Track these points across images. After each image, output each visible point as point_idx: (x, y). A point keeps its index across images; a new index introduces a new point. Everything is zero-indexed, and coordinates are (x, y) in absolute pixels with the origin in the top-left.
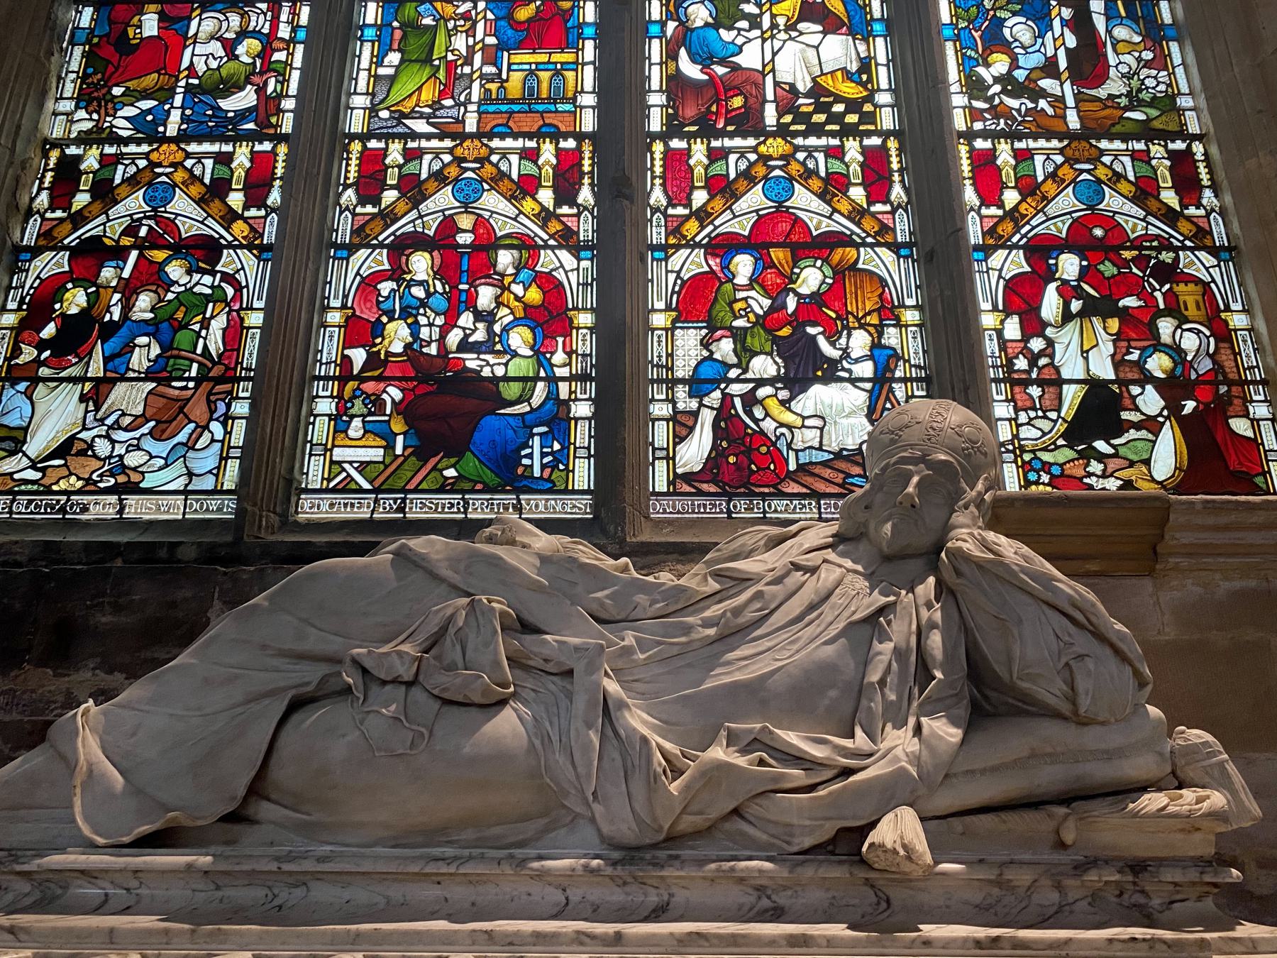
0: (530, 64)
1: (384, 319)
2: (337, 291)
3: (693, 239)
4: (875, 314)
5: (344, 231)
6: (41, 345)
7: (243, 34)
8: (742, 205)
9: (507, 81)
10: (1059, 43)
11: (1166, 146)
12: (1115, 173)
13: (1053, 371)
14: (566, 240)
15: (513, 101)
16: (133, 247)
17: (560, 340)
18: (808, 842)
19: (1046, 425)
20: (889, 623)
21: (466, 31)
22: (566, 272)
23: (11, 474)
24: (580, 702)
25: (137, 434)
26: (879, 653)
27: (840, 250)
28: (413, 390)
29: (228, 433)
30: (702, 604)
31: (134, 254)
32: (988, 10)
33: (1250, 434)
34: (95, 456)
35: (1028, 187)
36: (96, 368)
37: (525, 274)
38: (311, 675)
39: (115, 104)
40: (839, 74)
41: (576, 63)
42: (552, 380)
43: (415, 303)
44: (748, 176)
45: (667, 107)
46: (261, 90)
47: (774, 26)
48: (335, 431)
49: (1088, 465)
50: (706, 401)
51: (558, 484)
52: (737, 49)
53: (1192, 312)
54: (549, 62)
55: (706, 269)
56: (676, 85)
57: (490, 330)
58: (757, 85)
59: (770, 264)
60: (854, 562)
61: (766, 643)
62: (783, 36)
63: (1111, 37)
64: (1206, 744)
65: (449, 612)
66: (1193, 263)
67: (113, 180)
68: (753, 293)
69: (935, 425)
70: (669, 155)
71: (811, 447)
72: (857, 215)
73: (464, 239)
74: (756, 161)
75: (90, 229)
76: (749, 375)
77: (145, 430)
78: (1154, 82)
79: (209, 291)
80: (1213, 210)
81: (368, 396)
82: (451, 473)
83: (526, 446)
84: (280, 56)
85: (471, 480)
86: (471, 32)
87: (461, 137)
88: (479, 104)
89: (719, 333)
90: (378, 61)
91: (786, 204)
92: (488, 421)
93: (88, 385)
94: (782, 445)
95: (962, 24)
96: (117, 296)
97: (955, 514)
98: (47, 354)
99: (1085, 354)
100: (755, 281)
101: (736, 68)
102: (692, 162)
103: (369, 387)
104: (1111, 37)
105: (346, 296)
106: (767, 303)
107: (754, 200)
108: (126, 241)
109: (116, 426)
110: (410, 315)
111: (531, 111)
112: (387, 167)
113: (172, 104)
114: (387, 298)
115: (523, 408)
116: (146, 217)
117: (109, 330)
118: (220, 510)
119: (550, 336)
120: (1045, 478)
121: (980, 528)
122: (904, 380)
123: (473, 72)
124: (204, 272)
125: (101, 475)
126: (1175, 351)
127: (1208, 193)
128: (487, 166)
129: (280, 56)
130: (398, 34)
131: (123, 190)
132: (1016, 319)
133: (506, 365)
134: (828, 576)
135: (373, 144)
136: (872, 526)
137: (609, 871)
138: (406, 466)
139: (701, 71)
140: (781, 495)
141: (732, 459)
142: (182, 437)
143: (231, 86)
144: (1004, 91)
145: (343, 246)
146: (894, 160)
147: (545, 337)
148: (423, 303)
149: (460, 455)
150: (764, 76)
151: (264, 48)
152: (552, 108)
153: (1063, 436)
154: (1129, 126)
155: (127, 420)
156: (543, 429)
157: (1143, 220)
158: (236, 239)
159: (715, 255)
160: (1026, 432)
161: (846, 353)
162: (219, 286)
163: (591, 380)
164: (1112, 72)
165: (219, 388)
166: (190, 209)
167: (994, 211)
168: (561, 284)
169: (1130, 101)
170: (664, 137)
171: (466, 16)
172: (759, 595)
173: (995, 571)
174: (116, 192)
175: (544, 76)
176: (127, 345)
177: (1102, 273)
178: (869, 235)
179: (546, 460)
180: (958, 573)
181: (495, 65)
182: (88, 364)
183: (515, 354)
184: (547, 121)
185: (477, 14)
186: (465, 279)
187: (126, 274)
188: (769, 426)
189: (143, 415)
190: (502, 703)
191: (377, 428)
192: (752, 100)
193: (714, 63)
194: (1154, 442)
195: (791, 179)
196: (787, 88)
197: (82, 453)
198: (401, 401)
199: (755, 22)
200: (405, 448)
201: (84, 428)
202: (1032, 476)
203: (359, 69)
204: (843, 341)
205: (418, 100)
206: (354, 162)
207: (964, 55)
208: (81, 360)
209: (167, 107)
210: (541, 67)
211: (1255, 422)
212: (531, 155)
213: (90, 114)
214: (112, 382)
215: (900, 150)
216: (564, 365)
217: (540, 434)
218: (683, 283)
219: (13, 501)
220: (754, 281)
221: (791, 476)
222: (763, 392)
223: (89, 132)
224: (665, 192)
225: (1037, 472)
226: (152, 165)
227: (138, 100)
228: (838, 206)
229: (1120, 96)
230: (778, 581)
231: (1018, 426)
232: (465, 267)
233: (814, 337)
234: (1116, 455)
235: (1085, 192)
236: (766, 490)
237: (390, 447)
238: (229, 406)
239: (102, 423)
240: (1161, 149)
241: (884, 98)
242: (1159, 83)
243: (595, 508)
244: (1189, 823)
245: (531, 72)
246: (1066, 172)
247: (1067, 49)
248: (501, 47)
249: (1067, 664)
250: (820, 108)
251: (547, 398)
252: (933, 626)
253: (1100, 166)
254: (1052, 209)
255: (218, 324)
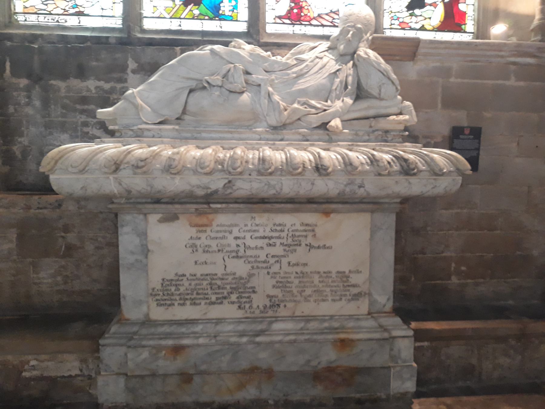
18: (315, 126)
20: (339, 73)
24: (263, 93)
26: (336, 82)
30: (292, 67)
38: (193, 84)
51: (234, 17)
60: (333, 56)
61: (308, 79)
64: (409, 105)
65: (228, 68)
69: (359, 15)
85: (203, 15)
97: (360, 43)
121: (367, 48)
134: (325, 60)
136: (338, 46)
137: (271, 131)
138: (180, 9)
172: (307, 65)
173: (367, 61)
180: (358, 61)
190: (243, 92)
230: (312, 61)
243: (249, 27)
244: (400, 122)
249: (380, 86)
252: (350, 75)
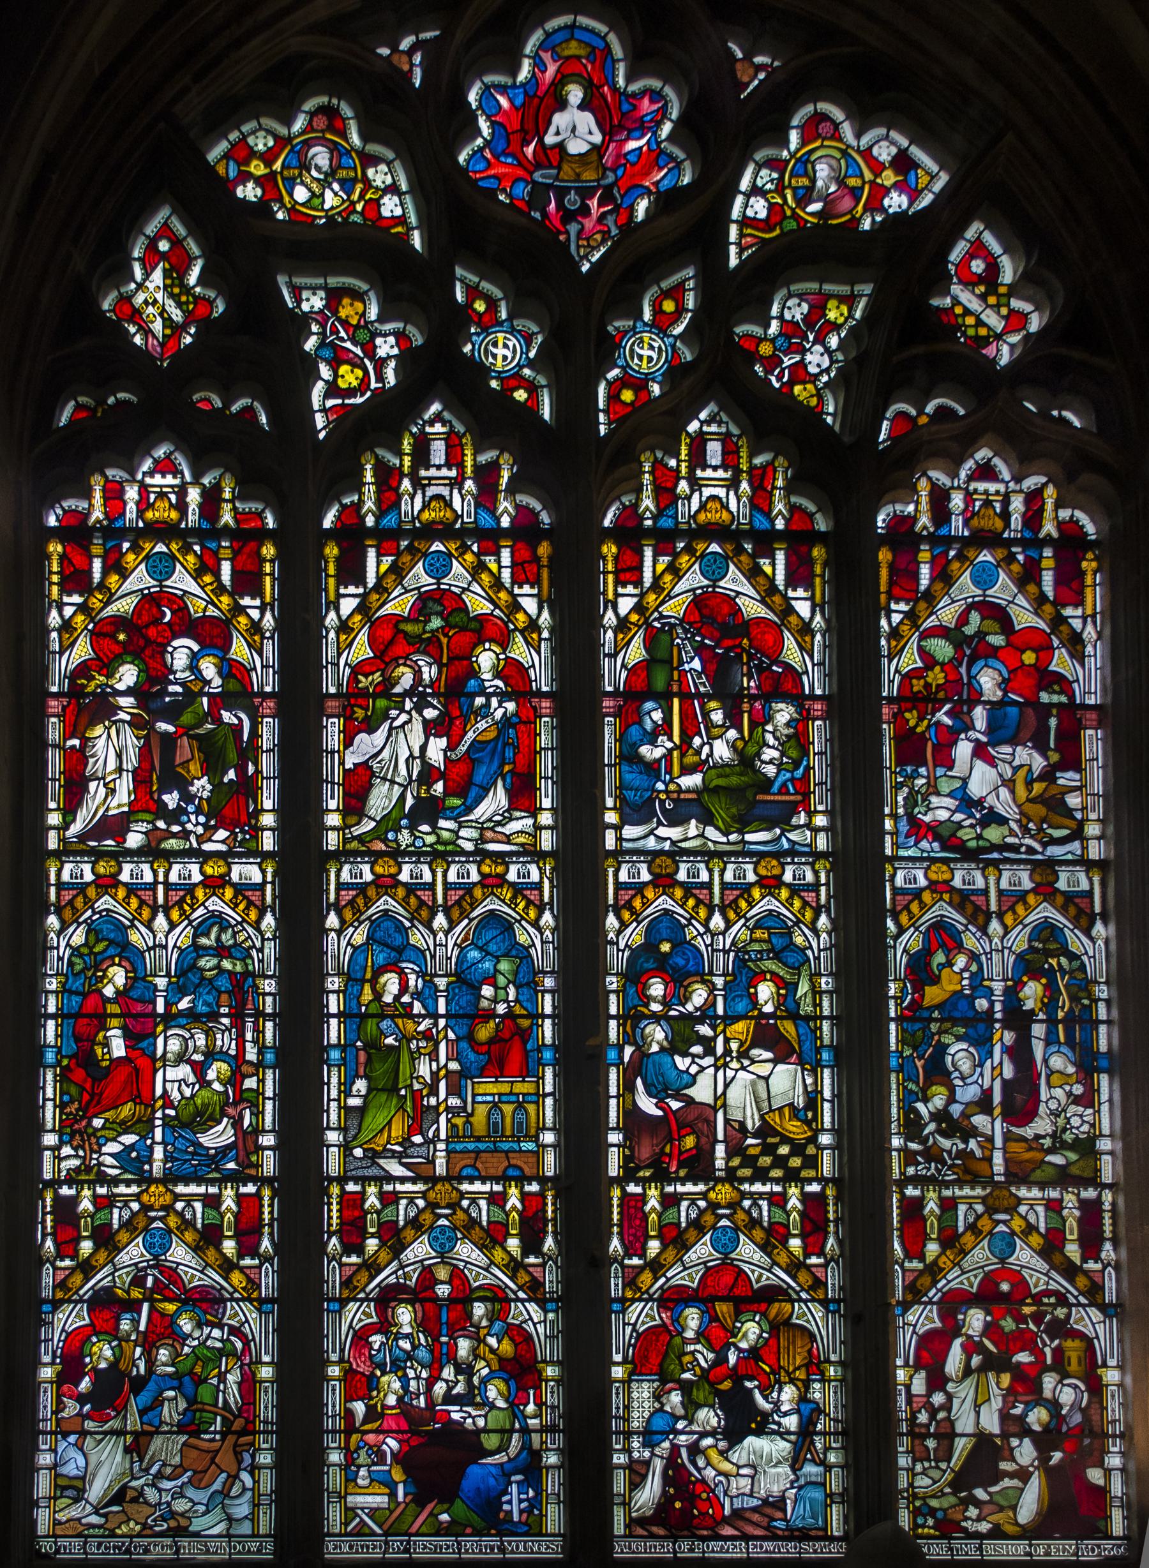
0: (493, 1095)
1: (378, 1373)
2: (334, 1343)
3: (647, 1292)
4: (803, 1369)
5: (334, 1282)
6: (81, 1399)
7: (211, 1054)
8: (691, 1256)
9: (472, 1115)
10: (996, 1072)
11: (1078, 1195)
12: (1028, 1224)
13: (948, 1424)
14: (534, 1292)
15: (478, 1139)
16: (144, 1300)
17: (532, 1392)
19: (936, 1474)
21: (429, 1054)
22: (535, 1324)
23: (79, 1520)
25: (179, 1482)
27: (776, 1305)
28: (407, 1441)
29: (256, 1482)
31: (146, 1306)
32: (933, 1034)
33: (1101, 1482)
34: (147, 1503)
35: (949, 1239)
36: (133, 1421)
37: (498, 1326)
39: (98, 1138)
40: (786, 1110)
41: (537, 1094)
42: (525, 1431)
43: (402, 1355)
44: (698, 1226)
45: (624, 1147)
46: (237, 1123)
47: (727, 1052)
48: (347, 1480)
49: (966, 1510)
50: (657, 1451)
52: (690, 1079)
53: (1074, 1367)
54: (511, 1093)
55: (658, 1322)
56: (633, 1118)
57: (469, 1382)
58: (707, 1121)
59: (714, 1318)
62: (735, 1065)
63: (1047, 1066)
66: (1082, 1318)
67: (111, 1224)
68: (699, 1347)
70: (625, 1197)
71: (743, 1494)
72: (795, 1267)
73: (443, 1290)
74: (706, 1209)
75: (102, 1279)
76: (695, 1428)
77: (185, 1479)
78: (1079, 1121)
79: (219, 1345)
80: (1109, 1264)
81: (371, 1447)
82: (445, 1517)
83: (505, 1492)
84: (250, 1083)
86: (434, 1056)
87: (432, 1180)
88: (447, 1141)
89: (669, 1385)
90: (346, 1090)
91: (733, 1256)
92: (473, 1470)
93: (129, 1439)
94: (720, 1491)
95: (907, 1053)
96: (138, 1350)
98: (87, 1407)
99: (977, 1407)
100: (702, 1335)
101: (690, 1101)
102: (647, 1208)
103: (371, 1438)
104: (1047, 1066)
105: (342, 1350)
106: (711, 1356)
107: (702, 1251)
108: (136, 1294)
109: (159, 1475)
110: (400, 1368)
111: (496, 1151)
112: (367, 1212)
113: (153, 1138)
114: (379, 1351)
115: (501, 1458)
116: (149, 1267)
117: (139, 1385)
118: (259, 1552)
119: (522, 1389)
120: (930, 1522)
122: (824, 1434)
123: (439, 1104)
124: (213, 1325)
125: (154, 1520)
126: (1054, 1405)
127: (1108, 1246)
128: (459, 1212)
129: (250, 1083)
130: (362, 1056)
131: (124, 1237)
132: (923, 1374)
133: (485, 1416)
135: (351, 1187)
138: (408, 1512)
139: (656, 1105)
140: (718, 1537)
141: (678, 1505)
142: (217, 1486)
143: (203, 1118)
144: (940, 1131)
145: (334, 1299)
146: (831, 1208)
147: (518, 1389)
148: (409, 1356)
149: (452, 1503)
150: (716, 1111)
151: (233, 1072)
152: (515, 1146)
153: (950, 1485)
154: (1050, 1171)
155: (169, 1470)
156: (519, 1477)
157: (1046, 1275)
158: (236, 1290)
159: (667, 1309)
160: (922, 1481)
161: (777, 1404)
162: (228, 1340)
163: (559, 1431)
164: (1042, 1109)
165: (243, 1440)
166: (188, 1257)
167: (916, 1265)
168: (530, 1336)
169: (1054, 1143)
170: (621, 1181)
171: (427, 1035)
174: (117, 1238)
175: (508, 1109)
176: (156, 1399)
177: (1002, 1328)
178: (803, 1289)
179: (523, 1505)
181: (460, 1097)
182: (125, 1418)
183: (493, 1406)
184: (513, 1162)
185: (438, 1032)
186: (444, 1331)
187: (142, 1327)
188: (710, 1473)
189: (181, 1465)
191: (381, 1477)
192: (704, 1140)
193: (669, 1096)
194: (1022, 1490)
195: (736, 1229)
196: (736, 1125)
197: (134, 1500)
198: (399, 1451)
199: (709, 1046)
200: (406, 1495)
201: (134, 1478)
202: (920, 1521)
203: (329, 1100)
204: (775, 1395)
205: (389, 1136)
206: (335, 1207)
207: (905, 1088)
208: (118, 1414)
209: (149, 1142)
210: (504, 1098)
211: (1108, 1472)
212: (496, 1200)
213: (75, 1149)
214: (151, 1435)
215: (838, 1198)
216: (534, 1417)
217: (518, 1482)
218: (639, 1335)
219: (85, 1543)
220: (701, 1335)
221: (726, 1521)
222: (708, 1442)
223: (77, 1170)
224: (622, 1241)
225: (924, 1516)
226: (146, 1208)
227: (120, 1134)
228: (778, 1259)
229: (1044, 1137)
231: (914, 1475)
232: (444, 1320)
233: (751, 1390)
234: (990, 1502)
235: (1000, 1244)
236: (705, 1533)
237: (393, 1495)
238: (253, 1457)
239: (147, 1471)
240: (1073, 1198)
241: (825, 1139)
242: (1084, 1122)
245: (495, 1105)
246: (985, 1224)
247: (1004, 1081)
248: (464, 1074)
250: (768, 1150)
251: (522, 1448)
253: (1016, 1217)
254: (967, 1262)
255: (233, 1378)
